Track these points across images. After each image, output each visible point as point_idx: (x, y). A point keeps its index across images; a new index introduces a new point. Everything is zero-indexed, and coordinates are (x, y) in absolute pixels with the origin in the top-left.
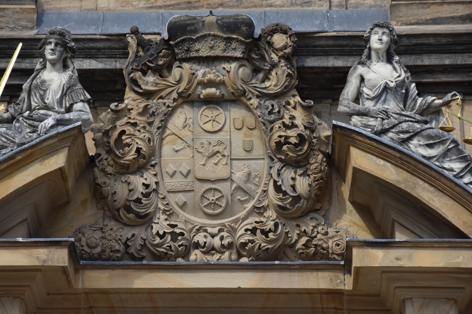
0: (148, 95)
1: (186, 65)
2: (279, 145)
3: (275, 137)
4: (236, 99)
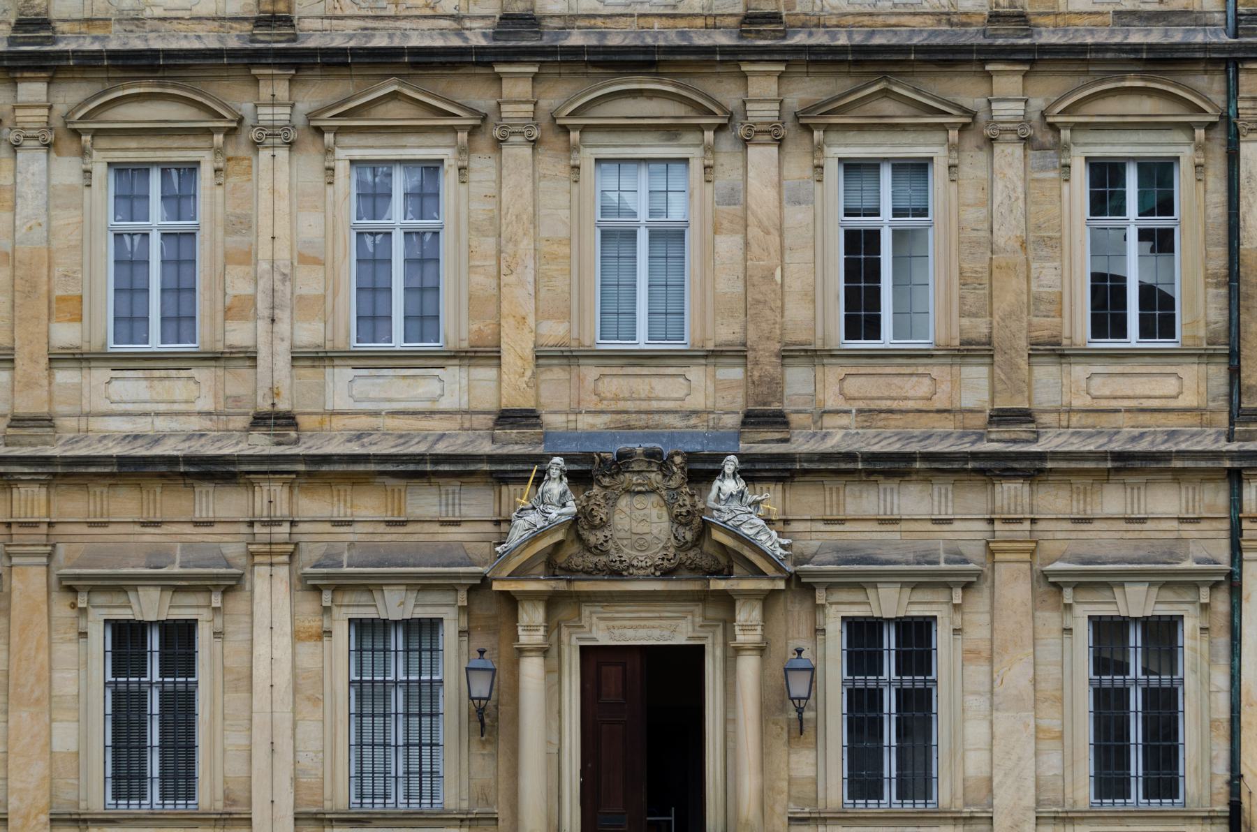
0: (606, 487)
1: (627, 475)
4: (653, 491)
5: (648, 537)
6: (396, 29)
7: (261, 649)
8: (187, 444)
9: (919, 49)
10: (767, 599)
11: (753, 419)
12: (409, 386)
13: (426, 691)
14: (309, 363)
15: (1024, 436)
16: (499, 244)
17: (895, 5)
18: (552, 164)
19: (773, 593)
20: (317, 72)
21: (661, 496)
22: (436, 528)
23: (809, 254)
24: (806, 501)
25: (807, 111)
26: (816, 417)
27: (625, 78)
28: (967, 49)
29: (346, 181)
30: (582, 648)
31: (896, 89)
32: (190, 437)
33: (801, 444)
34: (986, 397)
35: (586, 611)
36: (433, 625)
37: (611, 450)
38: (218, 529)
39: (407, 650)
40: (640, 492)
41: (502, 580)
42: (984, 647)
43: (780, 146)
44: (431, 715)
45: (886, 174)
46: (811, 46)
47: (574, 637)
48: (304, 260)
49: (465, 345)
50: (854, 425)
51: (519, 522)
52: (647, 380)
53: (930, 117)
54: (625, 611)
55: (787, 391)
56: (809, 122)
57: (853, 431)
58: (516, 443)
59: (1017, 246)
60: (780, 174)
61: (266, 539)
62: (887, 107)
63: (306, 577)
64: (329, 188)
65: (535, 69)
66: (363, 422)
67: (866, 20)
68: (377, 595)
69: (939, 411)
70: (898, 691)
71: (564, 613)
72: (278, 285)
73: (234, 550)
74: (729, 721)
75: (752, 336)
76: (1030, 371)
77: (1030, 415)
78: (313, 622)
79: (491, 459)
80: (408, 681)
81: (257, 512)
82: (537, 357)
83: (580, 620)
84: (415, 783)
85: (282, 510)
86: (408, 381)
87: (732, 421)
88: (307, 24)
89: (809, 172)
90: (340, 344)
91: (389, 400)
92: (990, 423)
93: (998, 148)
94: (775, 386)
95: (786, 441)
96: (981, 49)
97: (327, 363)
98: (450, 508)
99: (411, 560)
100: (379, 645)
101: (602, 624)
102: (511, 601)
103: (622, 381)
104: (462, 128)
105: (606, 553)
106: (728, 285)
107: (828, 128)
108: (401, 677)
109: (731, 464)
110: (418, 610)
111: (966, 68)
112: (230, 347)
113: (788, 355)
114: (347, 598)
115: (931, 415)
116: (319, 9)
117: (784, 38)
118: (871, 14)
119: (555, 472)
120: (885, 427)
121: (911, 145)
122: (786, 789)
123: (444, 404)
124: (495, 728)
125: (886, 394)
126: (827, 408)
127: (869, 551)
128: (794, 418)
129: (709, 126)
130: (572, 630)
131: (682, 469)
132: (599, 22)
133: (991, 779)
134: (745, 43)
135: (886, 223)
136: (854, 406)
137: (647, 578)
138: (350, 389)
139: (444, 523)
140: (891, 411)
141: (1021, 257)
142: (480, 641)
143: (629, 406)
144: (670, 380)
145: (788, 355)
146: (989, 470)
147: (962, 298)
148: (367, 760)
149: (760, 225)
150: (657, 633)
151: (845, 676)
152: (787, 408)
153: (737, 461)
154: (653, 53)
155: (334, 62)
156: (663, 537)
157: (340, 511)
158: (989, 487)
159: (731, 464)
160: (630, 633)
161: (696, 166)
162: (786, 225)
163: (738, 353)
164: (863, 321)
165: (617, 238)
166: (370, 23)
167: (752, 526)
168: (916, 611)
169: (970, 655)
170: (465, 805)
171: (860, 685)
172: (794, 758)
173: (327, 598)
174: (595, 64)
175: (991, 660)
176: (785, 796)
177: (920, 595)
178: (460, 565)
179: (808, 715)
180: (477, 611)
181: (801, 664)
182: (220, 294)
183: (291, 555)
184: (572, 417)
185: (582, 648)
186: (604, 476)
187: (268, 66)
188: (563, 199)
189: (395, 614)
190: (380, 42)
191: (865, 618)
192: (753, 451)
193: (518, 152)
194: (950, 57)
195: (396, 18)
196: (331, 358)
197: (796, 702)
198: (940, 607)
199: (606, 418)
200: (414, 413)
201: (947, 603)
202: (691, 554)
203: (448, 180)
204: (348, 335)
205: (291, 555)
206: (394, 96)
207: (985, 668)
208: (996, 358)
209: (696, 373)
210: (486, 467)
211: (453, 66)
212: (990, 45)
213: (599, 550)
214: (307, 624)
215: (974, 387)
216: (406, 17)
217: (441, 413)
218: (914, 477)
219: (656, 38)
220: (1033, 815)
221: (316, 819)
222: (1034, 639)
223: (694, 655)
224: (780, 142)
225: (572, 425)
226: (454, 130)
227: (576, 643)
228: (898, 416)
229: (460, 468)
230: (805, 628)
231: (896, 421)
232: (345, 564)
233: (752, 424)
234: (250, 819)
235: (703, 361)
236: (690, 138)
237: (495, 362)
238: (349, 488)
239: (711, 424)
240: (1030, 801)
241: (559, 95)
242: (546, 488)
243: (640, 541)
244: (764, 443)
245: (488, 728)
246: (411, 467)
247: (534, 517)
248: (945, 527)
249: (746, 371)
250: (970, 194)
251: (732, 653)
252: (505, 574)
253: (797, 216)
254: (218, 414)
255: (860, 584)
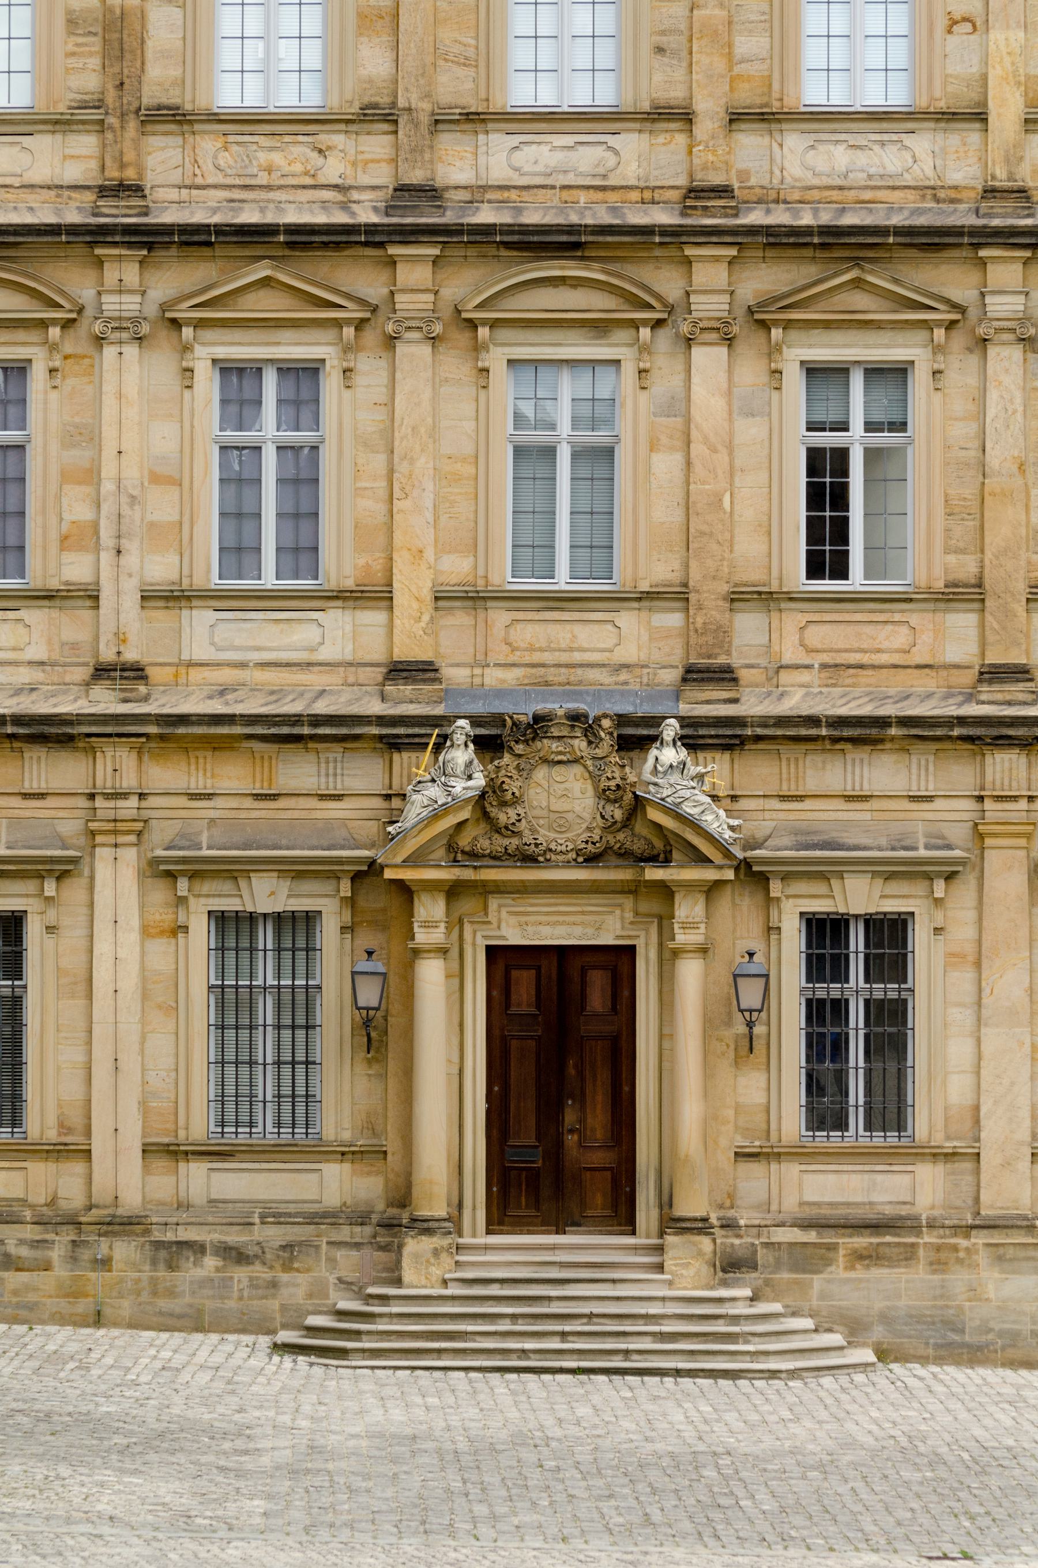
0: (520, 756)
1: (545, 741)
2: (604, 791)
3: (602, 786)
5: (570, 816)
6: (268, 201)
7: (103, 947)
8: (15, 700)
9: (898, 231)
10: (711, 890)
11: (694, 675)
12: (282, 632)
13: (301, 997)
14: (161, 603)
15: (1021, 697)
16: (390, 463)
17: (870, 177)
18: (455, 365)
19: (718, 884)
20: (173, 251)
21: (585, 767)
22: (314, 803)
23: (764, 476)
24: (759, 772)
25: (762, 305)
26: (771, 673)
27: (545, 264)
28: (957, 231)
29: (207, 385)
30: (489, 948)
31: (870, 278)
32: (18, 692)
33: (753, 705)
34: (973, 648)
35: (493, 903)
36: (310, 919)
37: (526, 710)
38: (50, 802)
39: (279, 950)
40: (560, 762)
41: (396, 866)
42: (970, 949)
43: (729, 346)
44: (307, 1027)
45: (857, 381)
46: (768, 227)
47: (479, 935)
48: (156, 479)
49: (349, 584)
50: (817, 682)
51: (416, 797)
52: (568, 627)
53: (912, 310)
54: (541, 905)
55: (736, 642)
56: (762, 318)
57: (816, 690)
58: (410, 702)
59: (1015, 468)
60: (730, 380)
61: (111, 814)
62: (860, 300)
63: (155, 861)
64: (187, 393)
65: (436, 251)
66: (226, 676)
67: (835, 195)
68: (243, 883)
69: (918, 667)
70: (867, 1002)
71: (467, 905)
72: (126, 510)
73: (70, 827)
74: (666, 1035)
75: (695, 577)
76: (1029, 620)
77: (1027, 672)
78: (163, 916)
79: (381, 720)
80: (279, 987)
81: (99, 782)
82: (437, 598)
83: (486, 914)
84: (287, 1107)
85: (129, 780)
86: (281, 626)
87: (671, 676)
88: (161, 194)
89: (764, 378)
90: (199, 582)
91: (258, 649)
92: (980, 681)
93: (992, 351)
94: (722, 634)
95: (736, 701)
96: (974, 232)
97: (183, 603)
98: (331, 779)
99: (284, 842)
100: (245, 943)
101: (513, 920)
102: (405, 891)
103: (538, 628)
104: (348, 321)
105: (517, 834)
106: (665, 512)
107: (788, 325)
108: (271, 981)
109: (671, 729)
110: (292, 901)
111: (955, 253)
112: (67, 583)
113: (736, 598)
114: (207, 886)
115: (909, 671)
116: (176, 177)
117: (736, 216)
118: (841, 188)
119: (459, 738)
120: (854, 685)
121: (888, 346)
122: (732, 1119)
123: (325, 654)
124: (383, 1044)
125: (856, 645)
126: (784, 662)
127: (834, 834)
128: (743, 674)
129: (645, 322)
130: (476, 926)
131: (611, 734)
132: (513, 195)
133: (977, 1108)
134: (688, 221)
135: (856, 439)
136: (817, 660)
137: (567, 865)
138: (212, 635)
139: (322, 797)
140: (861, 667)
141: (1019, 481)
142: (367, 939)
143: (547, 657)
144: (596, 627)
145: (736, 598)
146: (979, 738)
147: (947, 530)
148: (230, 1080)
149: (706, 440)
150: (578, 930)
151: (804, 984)
152: (735, 661)
153: (677, 725)
154: (579, 233)
155: (195, 239)
156: (587, 816)
157: (199, 782)
158: (978, 758)
159: (671, 729)
160: (546, 930)
161: (629, 370)
162: (736, 442)
163: (679, 596)
164: (827, 557)
165: (532, 458)
166: (237, 194)
167: (696, 804)
168: (891, 906)
169: (954, 959)
170: (346, 1136)
171: (821, 994)
172: (742, 1081)
173: (183, 886)
174: (507, 245)
175: (978, 964)
176: (730, 1127)
177: (895, 887)
178: (343, 848)
179: (759, 1030)
180: (361, 902)
181: (753, 969)
182: (53, 520)
183: (139, 834)
184: (477, 671)
185: (489, 948)
186: (517, 742)
187: (115, 244)
188: (469, 409)
189: (264, 906)
190: (249, 216)
191: (828, 914)
192: (696, 713)
193: (414, 352)
194: (937, 240)
195: (269, 188)
196: (189, 598)
197: (747, 1014)
198: (918, 902)
199: (518, 672)
200: (288, 665)
201: (927, 897)
202: (621, 836)
203: (331, 384)
204: (209, 571)
205: (139, 834)
206: (266, 282)
207: (970, 975)
208: (988, 603)
209: (628, 619)
210: (375, 731)
211: (338, 246)
212: (985, 227)
213: (509, 830)
214: (158, 917)
215: (958, 638)
216: (280, 187)
217: (320, 664)
218: (888, 746)
219: (582, 214)
220: (1028, 1152)
221: (169, 1152)
222: (1031, 940)
223: (621, 958)
224: (729, 341)
225: (477, 681)
226: (338, 324)
227: (482, 943)
228: (870, 672)
229: (344, 731)
230: (756, 927)
231: (867, 677)
232: (205, 845)
233: (695, 680)
234: (90, 1151)
235: (636, 605)
236: (623, 335)
237: (385, 604)
238: (209, 754)
239: (645, 680)
240: (1024, 1133)
241: (467, 284)
242: (449, 756)
243: (559, 821)
244: (707, 704)
245: (374, 1044)
246: (285, 730)
247: (434, 792)
248: (925, 806)
249: (688, 617)
250: (960, 406)
251: (669, 957)
252: (399, 860)
253: (750, 431)
254: (53, 664)
255: (822, 873)
